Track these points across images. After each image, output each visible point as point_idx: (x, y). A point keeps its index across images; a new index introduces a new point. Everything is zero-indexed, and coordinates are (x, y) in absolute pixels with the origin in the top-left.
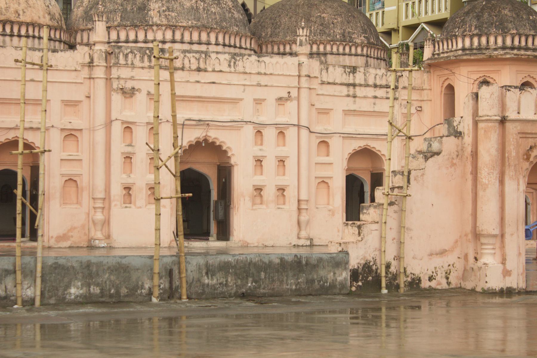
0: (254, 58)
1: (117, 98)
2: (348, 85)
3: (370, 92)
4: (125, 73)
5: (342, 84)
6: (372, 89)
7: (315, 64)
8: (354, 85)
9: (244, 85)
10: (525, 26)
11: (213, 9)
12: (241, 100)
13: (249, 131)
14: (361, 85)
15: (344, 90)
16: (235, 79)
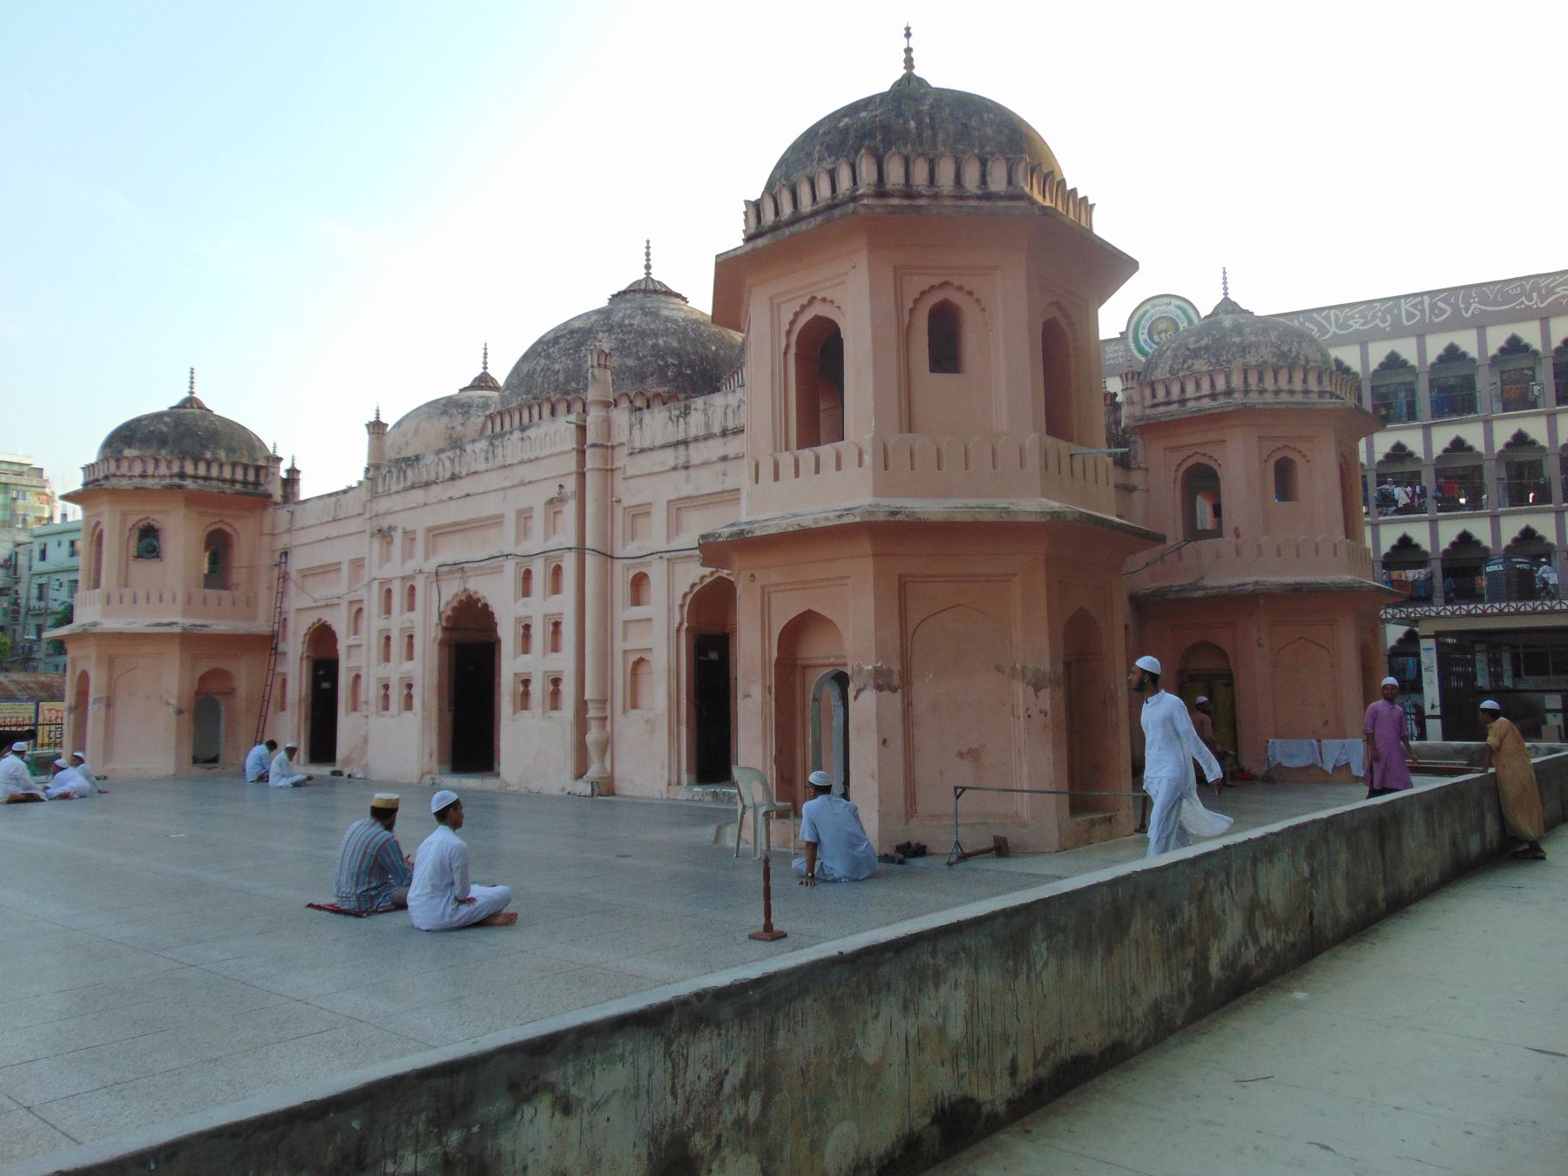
0: (517, 434)
1: (376, 543)
2: (676, 444)
3: (715, 449)
4: (382, 505)
5: (662, 447)
6: (720, 441)
7: (621, 416)
8: (686, 443)
9: (504, 489)
10: (809, 155)
11: (557, 367)
12: (502, 516)
13: (510, 571)
14: (696, 439)
15: (669, 457)
16: (492, 481)
